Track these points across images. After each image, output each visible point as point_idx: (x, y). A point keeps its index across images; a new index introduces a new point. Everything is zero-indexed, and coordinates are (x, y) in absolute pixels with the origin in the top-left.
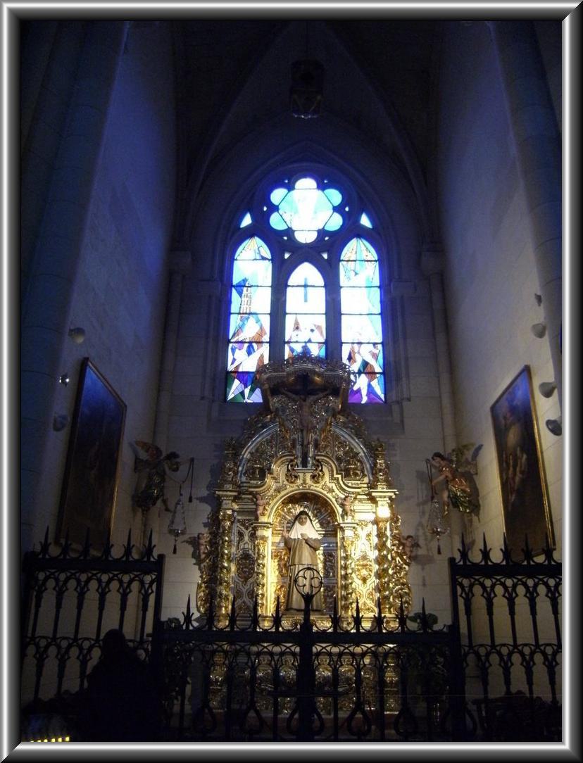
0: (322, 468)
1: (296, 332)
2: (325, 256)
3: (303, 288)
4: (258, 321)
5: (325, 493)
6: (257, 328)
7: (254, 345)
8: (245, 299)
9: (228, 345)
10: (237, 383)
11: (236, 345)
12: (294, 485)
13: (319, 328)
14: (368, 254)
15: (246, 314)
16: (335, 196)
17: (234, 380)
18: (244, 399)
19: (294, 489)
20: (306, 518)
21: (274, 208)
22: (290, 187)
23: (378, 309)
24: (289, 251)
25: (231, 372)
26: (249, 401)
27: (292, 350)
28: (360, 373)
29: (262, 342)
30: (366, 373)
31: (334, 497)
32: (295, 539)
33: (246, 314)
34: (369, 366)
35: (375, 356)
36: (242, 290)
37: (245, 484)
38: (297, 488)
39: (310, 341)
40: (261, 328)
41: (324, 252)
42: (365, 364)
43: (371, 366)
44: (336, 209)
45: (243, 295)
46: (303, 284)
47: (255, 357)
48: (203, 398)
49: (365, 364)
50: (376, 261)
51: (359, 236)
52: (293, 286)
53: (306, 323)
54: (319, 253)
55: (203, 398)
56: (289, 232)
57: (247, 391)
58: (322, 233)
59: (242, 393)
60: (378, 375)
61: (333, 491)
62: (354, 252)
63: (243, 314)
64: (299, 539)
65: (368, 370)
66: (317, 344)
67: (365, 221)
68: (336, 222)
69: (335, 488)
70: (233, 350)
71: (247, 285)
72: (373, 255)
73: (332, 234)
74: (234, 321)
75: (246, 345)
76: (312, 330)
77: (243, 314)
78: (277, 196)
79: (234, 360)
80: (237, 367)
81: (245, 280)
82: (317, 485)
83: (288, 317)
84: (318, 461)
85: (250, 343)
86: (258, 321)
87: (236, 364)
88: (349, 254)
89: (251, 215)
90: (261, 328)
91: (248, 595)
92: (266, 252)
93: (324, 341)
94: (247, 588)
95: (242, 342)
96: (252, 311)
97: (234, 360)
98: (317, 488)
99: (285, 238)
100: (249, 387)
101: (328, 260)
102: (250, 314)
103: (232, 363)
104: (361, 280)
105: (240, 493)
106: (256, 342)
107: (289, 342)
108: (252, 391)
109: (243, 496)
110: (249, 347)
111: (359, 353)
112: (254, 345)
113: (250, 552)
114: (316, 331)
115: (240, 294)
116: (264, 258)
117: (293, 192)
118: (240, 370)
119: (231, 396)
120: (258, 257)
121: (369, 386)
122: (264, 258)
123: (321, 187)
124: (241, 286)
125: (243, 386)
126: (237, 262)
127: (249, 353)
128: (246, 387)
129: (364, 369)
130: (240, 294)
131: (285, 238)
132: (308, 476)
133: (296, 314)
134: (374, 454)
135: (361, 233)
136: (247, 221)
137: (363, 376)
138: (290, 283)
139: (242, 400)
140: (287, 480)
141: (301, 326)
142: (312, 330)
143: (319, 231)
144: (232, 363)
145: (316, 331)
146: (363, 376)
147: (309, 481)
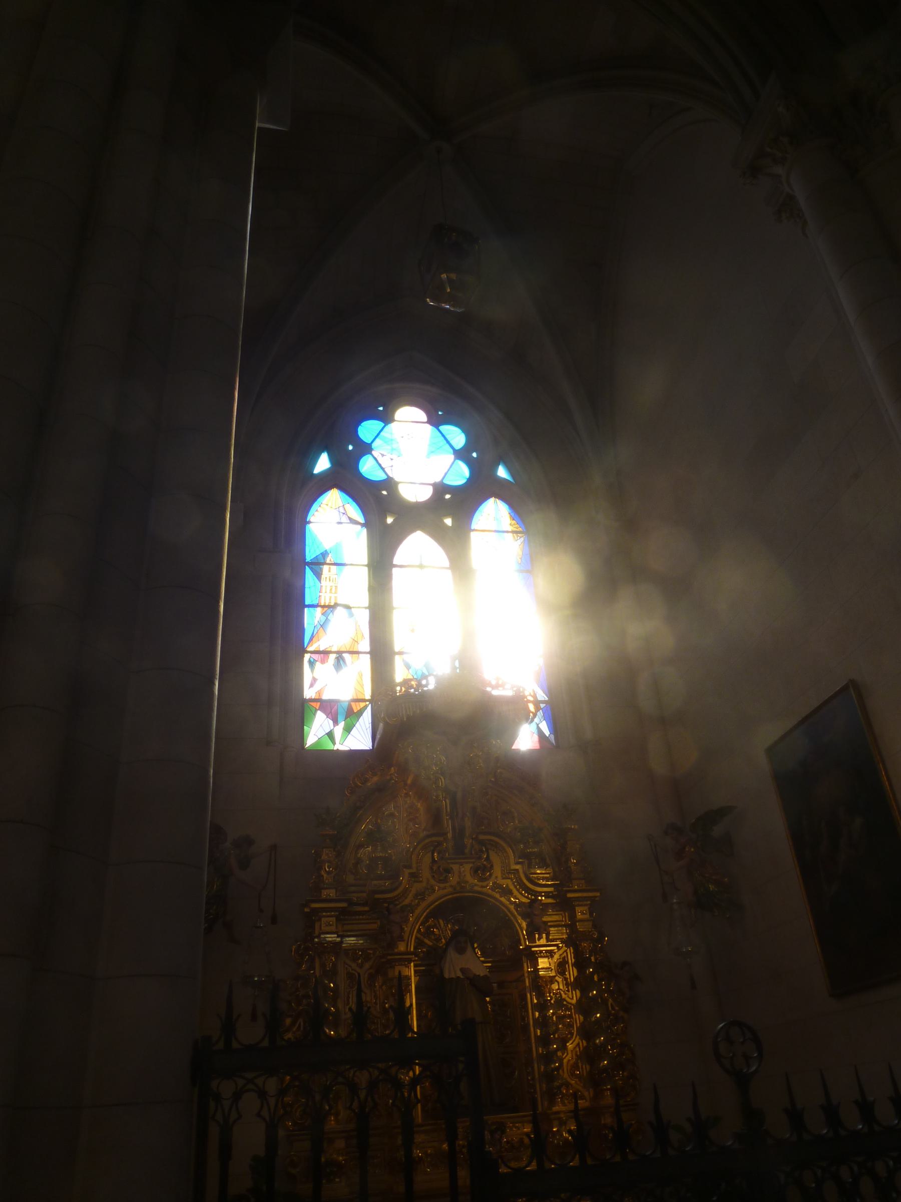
0: (488, 856)
5: (497, 896)
11: (315, 656)
16: (457, 437)
17: (315, 714)
19: (445, 891)
22: (387, 418)
25: (311, 700)
36: (321, 570)
45: (323, 576)
46: (418, 564)
56: (389, 484)
61: (510, 893)
68: (460, 474)
70: (312, 664)
75: (332, 657)
78: (367, 430)
79: (314, 680)
81: (325, 554)
82: (485, 884)
89: (329, 455)
92: (358, 516)
95: (326, 653)
97: (314, 680)
103: (312, 686)
110: (337, 658)
115: (318, 575)
117: (392, 426)
120: (344, 519)
122: (353, 521)
123: (435, 421)
124: (317, 565)
125: (331, 722)
126: (311, 524)
132: (468, 867)
135: (500, 491)
136: (323, 463)
140: (433, 877)
144: (312, 686)
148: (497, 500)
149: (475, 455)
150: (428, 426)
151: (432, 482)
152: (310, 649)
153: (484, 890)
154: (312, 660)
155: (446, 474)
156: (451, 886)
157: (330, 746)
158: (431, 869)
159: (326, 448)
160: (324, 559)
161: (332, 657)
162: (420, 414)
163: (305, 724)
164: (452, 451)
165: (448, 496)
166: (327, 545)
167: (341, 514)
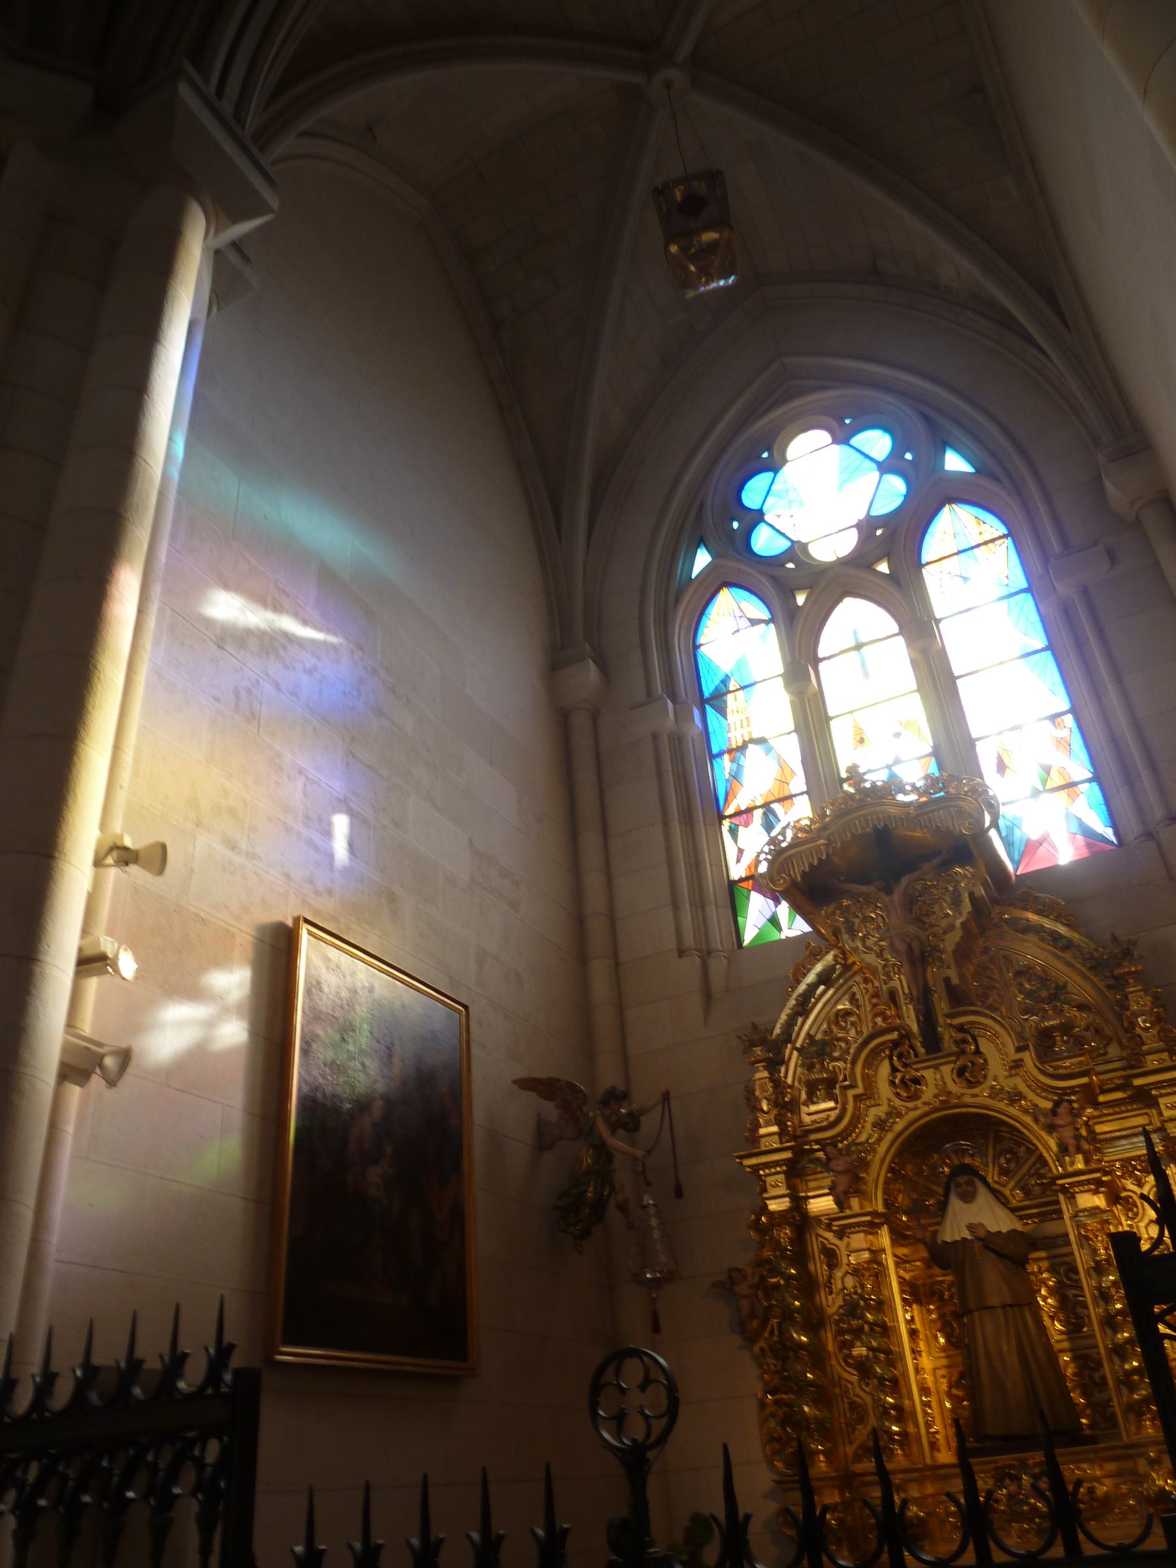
2: (883, 567)
3: (854, 653)
5: (1001, 1105)
9: (720, 824)
14: (983, 527)
16: (878, 442)
19: (918, 1113)
20: (970, 1183)
21: (758, 516)
23: (1041, 641)
25: (741, 880)
29: (790, 797)
31: (1025, 1111)
32: (956, 1242)
40: (782, 764)
41: (879, 560)
44: (884, 467)
45: (729, 710)
46: (852, 644)
50: (1005, 536)
54: (869, 567)
55: (681, 953)
56: (797, 551)
64: (965, 1239)
66: (916, 761)
67: (955, 462)
69: (1022, 1088)
70: (733, 832)
72: (994, 527)
73: (886, 521)
75: (758, 814)
81: (725, 681)
82: (976, 1091)
90: (782, 764)
92: (760, 611)
98: (979, 1098)
99: (790, 565)
101: (892, 578)
106: (781, 800)
110: (765, 814)
115: (722, 712)
116: (754, 622)
119: (748, 937)
122: (754, 622)
123: (842, 437)
124: (718, 700)
131: (790, 565)
132: (947, 1070)
133: (851, 712)
134: (1114, 977)
138: (821, 653)
140: (898, 1095)
143: (859, 526)
148: (953, 505)
149: (908, 456)
150: (834, 446)
151: (855, 522)
152: (727, 813)
153: (978, 1100)
154: (733, 826)
155: (871, 503)
156: (925, 1103)
157: (776, 936)
158: (892, 1083)
159: (701, 541)
160: (726, 687)
162: (819, 437)
163: (738, 914)
164: (874, 466)
165: (879, 532)
166: (726, 667)
167: (738, 619)
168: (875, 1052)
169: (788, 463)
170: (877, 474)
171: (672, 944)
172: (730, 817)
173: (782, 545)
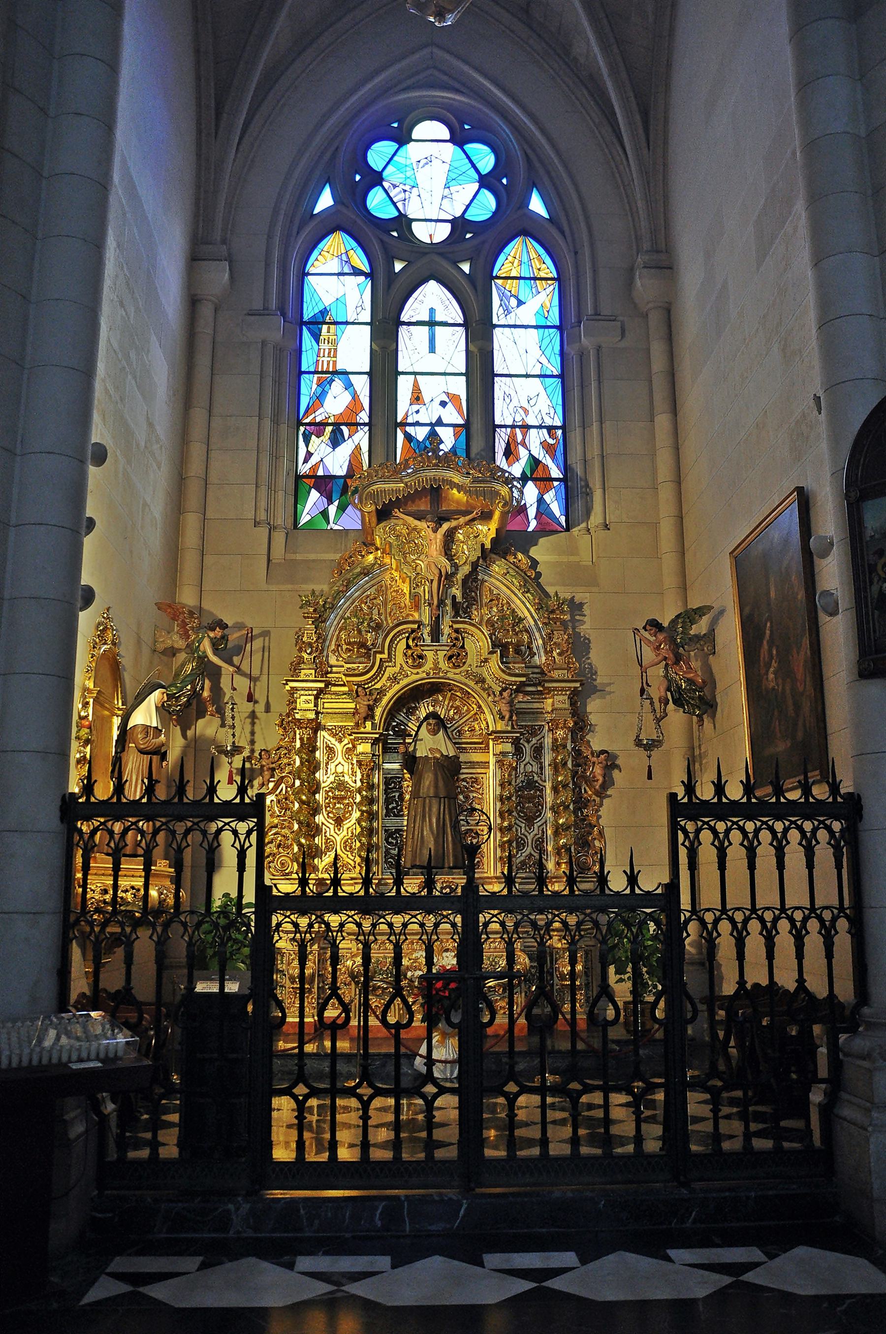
1: (415, 407)
4: (349, 386)
6: (346, 398)
7: (345, 429)
8: (324, 346)
10: (314, 495)
12: (420, 670)
13: (455, 398)
15: (327, 372)
17: (309, 493)
18: (328, 523)
21: (376, 179)
24: (401, 259)
26: (336, 527)
27: (409, 438)
28: (524, 479)
30: (534, 480)
33: (327, 372)
34: (540, 467)
35: (549, 449)
36: (320, 330)
37: (334, 669)
38: (424, 675)
39: (439, 422)
41: (463, 261)
42: (535, 462)
43: (546, 467)
47: (345, 450)
48: (256, 524)
49: (535, 462)
51: (525, 233)
52: (409, 324)
53: (431, 388)
57: (332, 510)
58: (459, 224)
59: (325, 514)
60: (556, 483)
62: (516, 263)
63: (322, 372)
65: (539, 473)
71: (327, 320)
74: (308, 386)
75: (329, 429)
76: (443, 404)
77: (322, 372)
79: (309, 455)
80: (315, 467)
81: (324, 312)
82: (458, 671)
83: (401, 379)
84: (457, 631)
85: (337, 425)
86: (349, 386)
87: (313, 461)
88: (507, 266)
90: (355, 397)
91: (345, 848)
93: (462, 422)
94: (342, 836)
95: (323, 424)
96: (339, 367)
97: (309, 455)
100: (336, 503)
102: (335, 373)
103: (306, 461)
104: (527, 314)
105: (328, 684)
106: (346, 424)
107: (404, 424)
108: (342, 508)
109: (334, 689)
111: (523, 444)
112: (344, 428)
113: (347, 778)
114: (450, 406)
115: (316, 337)
116: (357, 272)
117: (411, 148)
118: (320, 473)
121: (540, 501)
125: (325, 500)
127: (336, 441)
128: (330, 502)
129: (532, 472)
130: (316, 337)
133: (415, 374)
136: (325, 200)
137: (530, 484)
138: (404, 317)
139: (324, 526)
141: (426, 397)
142: (443, 404)
143: (454, 222)
144: (306, 461)
145: (450, 406)
146: (530, 484)
147: (444, 665)
150: (450, 145)
153: (457, 677)
154: (307, 433)
161: (329, 429)
168: (400, 633)
169: (412, 143)
170: (477, 185)
171: (251, 515)
172: (306, 424)
173: (389, 213)
